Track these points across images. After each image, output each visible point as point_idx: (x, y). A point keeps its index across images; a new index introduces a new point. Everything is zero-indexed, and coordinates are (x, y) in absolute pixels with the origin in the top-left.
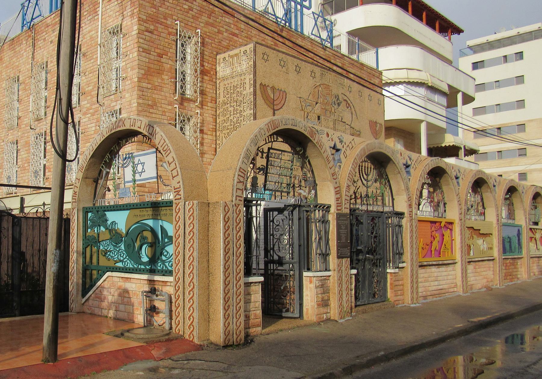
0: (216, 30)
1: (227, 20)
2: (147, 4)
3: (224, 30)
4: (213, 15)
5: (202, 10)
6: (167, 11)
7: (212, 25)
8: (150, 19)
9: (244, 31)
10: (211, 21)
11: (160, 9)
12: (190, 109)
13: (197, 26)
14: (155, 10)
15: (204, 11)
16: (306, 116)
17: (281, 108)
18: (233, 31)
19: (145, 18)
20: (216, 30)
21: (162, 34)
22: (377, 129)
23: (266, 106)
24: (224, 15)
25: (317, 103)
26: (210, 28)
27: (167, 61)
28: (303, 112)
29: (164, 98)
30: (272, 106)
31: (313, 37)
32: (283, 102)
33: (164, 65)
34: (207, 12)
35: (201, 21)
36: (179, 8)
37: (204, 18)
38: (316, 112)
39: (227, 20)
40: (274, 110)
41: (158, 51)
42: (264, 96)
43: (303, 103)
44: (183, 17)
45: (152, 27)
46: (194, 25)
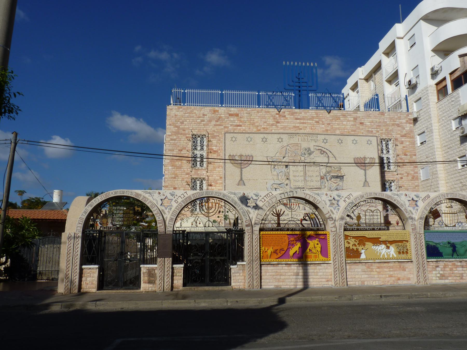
0: (223, 127)
1: (232, 119)
2: (172, 127)
6: (185, 127)
10: (218, 123)
18: (238, 124)
19: (170, 134)
20: (223, 127)
21: (182, 139)
25: (284, 157)
26: (217, 127)
37: (213, 123)
39: (232, 119)
40: (241, 168)
41: (179, 148)
44: (197, 126)
45: (175, 137)
46: (205, 129)
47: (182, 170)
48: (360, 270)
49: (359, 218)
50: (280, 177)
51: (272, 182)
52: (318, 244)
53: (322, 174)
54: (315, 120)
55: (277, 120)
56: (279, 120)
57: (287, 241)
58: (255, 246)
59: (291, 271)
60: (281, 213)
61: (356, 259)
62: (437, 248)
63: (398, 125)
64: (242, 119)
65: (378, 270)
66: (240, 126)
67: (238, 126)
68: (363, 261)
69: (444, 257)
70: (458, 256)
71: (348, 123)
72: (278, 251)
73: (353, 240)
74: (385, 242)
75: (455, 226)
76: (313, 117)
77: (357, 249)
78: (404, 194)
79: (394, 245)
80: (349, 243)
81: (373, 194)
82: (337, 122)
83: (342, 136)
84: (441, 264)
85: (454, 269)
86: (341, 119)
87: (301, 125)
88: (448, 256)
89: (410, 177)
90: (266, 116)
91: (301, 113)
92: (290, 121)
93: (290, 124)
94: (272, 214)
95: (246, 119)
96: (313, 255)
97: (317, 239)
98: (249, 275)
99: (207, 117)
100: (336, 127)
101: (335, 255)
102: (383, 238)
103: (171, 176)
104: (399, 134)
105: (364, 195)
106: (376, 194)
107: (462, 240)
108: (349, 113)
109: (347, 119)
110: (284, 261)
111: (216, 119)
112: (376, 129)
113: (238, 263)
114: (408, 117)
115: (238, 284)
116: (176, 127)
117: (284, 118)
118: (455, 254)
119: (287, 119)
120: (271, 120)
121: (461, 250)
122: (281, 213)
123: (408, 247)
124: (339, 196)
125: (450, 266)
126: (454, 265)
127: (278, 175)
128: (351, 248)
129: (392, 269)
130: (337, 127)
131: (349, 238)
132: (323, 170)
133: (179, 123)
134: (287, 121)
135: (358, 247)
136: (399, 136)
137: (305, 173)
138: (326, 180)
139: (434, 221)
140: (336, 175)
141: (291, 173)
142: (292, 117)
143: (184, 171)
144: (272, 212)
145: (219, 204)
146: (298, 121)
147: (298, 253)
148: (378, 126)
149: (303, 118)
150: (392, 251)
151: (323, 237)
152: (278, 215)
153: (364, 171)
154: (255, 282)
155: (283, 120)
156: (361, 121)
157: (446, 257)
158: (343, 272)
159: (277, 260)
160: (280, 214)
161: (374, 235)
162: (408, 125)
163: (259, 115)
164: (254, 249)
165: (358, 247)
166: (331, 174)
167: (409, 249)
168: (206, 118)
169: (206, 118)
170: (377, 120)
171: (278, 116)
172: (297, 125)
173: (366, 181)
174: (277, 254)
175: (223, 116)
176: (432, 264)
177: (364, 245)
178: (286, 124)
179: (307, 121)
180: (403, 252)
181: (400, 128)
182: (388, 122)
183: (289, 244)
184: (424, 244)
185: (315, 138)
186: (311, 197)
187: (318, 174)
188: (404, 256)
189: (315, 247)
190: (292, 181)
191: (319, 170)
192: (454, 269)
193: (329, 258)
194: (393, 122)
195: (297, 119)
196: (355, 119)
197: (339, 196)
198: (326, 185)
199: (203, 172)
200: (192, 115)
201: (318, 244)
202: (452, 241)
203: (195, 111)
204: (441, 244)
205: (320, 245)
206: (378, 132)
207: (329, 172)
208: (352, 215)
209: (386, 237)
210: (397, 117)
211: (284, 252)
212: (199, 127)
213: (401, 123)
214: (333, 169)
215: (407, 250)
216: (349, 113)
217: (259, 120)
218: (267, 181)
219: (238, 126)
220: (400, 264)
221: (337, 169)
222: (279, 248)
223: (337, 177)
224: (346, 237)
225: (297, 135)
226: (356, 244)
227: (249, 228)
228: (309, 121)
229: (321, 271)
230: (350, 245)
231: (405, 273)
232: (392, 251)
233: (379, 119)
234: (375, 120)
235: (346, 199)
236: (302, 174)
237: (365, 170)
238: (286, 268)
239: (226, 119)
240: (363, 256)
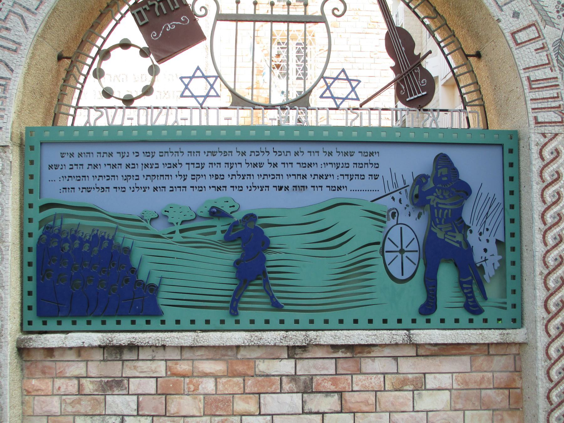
62: (126, 253)
69: (170, 314)
70: (277, 306)
75: (302, 101)
84: (145, 375)
85: (240, 405)
88: (200, 315)
107: (326, 196)
118: (254, 292)
121: (299, 264)
125: (208, 385)
139: (153, 71)
157: (185, 315)
176: (78, 369)
202: (248, 203)
204: (159, 228)
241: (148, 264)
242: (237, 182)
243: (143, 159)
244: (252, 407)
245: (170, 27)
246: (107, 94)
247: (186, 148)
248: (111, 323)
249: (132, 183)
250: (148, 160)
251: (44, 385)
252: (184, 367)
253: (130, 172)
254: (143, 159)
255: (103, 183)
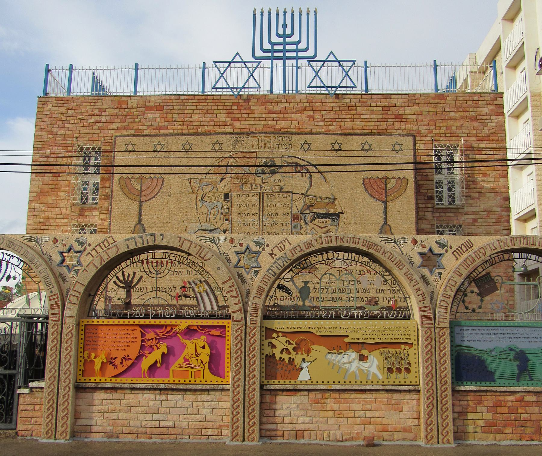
1: (150, 116)
2: (44, 133)
3: (145, 127)
4: (130, 117)
5: (113, 117)
6: (67, 132)
7: (126, 128)
8: (46, 146)
9: (178, 120)
10: (124, 124)
11: (59, 133)
12: (92, 217)
13: (105, 135)
14: (52, 136)
15: (116, 117)
16: (200, 197)
17: (154, 197)
18: (160, 124)
22: (388, 187)
23: (127, 200)
24: (146, 112)
27: (64, 178)
28: (194, 196)
29: (58, 213)
30: (138, 198)
31: (315, 91)
32: (156, 190)
33: (61, 182)
34: (121, 117)
35: (111, 128)
36: (81, 125)
37: (116, 124)
38: (221, 190)
39: (150, 116)
40: (141, 202)
42: (126, 190)
43: (194, 185)
44: (87, 132)
46: (101, 135)
47: (58, 209)
48: (294, 406)
49: (305, 292)
50: (212, 217)
51: (198, 226)
52: (203, 347)
53: (295, 211)
54: (306, 112)
55: (234, 116)
56: (239, 116)
57: (139, 339)
58: (66, 349)
59: (143, 403)
60: (135, 281)
61: (287, 382)
63: (474, 119)
64: (170, 116)
65: (336, 407)
66: (166, 128)
67: (160, 128)
68: (302, 387)
69: (498, 381)
71: (372, 116)
72: (117, 362)
73: (284, 340)
74: (358, 345)
76: (305, 108)
77: (291, 361)
78: (410, 239)
79: (378, 352)
80: (274, 346)
81: (334, 239)
82: (349, 116)
83: (340, 137)
85: (520, 411)
86: (358, 109)
87: (279, 123)
88: (507, 382)
89: (492, 219)
90: (215, 107)
91: (281, 102)
92: (258, 115)
93: (260, 122)
94: (115, 282)
95: (176, 116)
96: (190, 370)
97: (203, 337)
98: (48, 409)
99: (107, 114)
100: (346, 124)
101: (237, 373)
102: (353, 337)
103: (37, 221)
104: (473, 136)
105: (314, 241)
106: (342, 240)
108: (374, 97)
109: (371, 108)
110: (125, 380)
111: (121, 117)
112: (426, 128)
113: (31, 384)
114: (496, 102)
115: (31, 426)
116: (51, 133)
117: (249, 111)
119: (253, 112)
120: (222, 115)
122: (135, 281)
123: (411, 359)
124: (258, 244)
125: (509, 404)
126: (522, 400)
127: (208, 213)
128: (278, 356)
129: (369, 407)
130: (350, 124)
131: (275, 335)
132: (297, 203)
133: (55, 126)
134: (254, 115)
135: (293, 355)
136: (474, 139)
137: (262, 209)
138: (302, 222)
139: (482, 300)
140: (324, 211)
141: (235, 210)
142: (263, 108)
143: (61, 212)
144: (115, 279)
145: (8, 262)
146: (274, 115)
147: (159, 365)
148: (430, 120)
149: (285, 111)
150: (374, 366)
151: (218, 333)
152: (128, 286)
153: (383, 205)
154: (59, 424)
155: (245, 115)
156: (397, 113)
157: (502, 381)
158: (254, 410)
159: (114, 380)
160: (132, 281)
161: (323, 330)
162: (493, 117)
163: (201, 107)
164: (63, 355)
165: (293, 355)
166: (315, 211)
167: (412, 363)
168: (105, 116)
169: (105, 116)
170: (430, 109)
171: (235, 107)
172: (271, 123)
173: (385, 222)
174: (115, 366)
175: (135, 110)
177: (308, 351)
178: (251, 123)
179: (290, 116)
180: (399, 370)
181: (476, 124)
182: (452, 113)
183: (142, 347)
184: (448, 351)
185: (285, 139)
186: (193, 245)
187: (287, 210)
188: (401, 378)
189: (197, 355)
190: (235, 225)
191: (290, 203)
192: (520, 411)
193: (227, 379)
194: (462, 113)
195: (271, 112)
196: (386, 109)
197: (258, 244)
198: (302, 231)
199: (94, 213)
200: (80, 111)
201: (203, 347)
203: (85, 104)
205: (207, 350)
206: (431, 132)
207: (309, 207)
208: (289, 285)
209: (361, 334)
210: (471, 102)
211: (129, 363)
212: (91, 132)
213: (480, 114)
214: (319, 200)
215: (409, 364)
216: (374, 97)
217: (201, 116)
218: (186, 224)
219: (160, 128)
220: (389, 395)
221: (327, 201)
222: (120, 355)
223: (326, 216)
224: (268, 333)
225: (250, 136)
226: (291, 348)
227: (56, 311)
228: (294, 116)
229: (207, 404)
230: (274, 350)
231: (401, 415)
232: (374, 366)
233: (435, 107)
234: (426, 109)
235: (276, 251)
236: (256, 210)
237: (385, 202)
238: (132, 396)
239: (139, 117)
240: (304, 376)
241: (492, 365)
242: (515, 339)
243: (486, 332)
244: (523, 411)
245: (487, 286)
246: (467, 308)
247: (499, 328)
248: (478, 383)
249: (483, 339)
250: (488, 332)
251: (458, 403)
252: (501, 398)
253: (481, 336)
254: (486, 332)
255: (474, 339)
